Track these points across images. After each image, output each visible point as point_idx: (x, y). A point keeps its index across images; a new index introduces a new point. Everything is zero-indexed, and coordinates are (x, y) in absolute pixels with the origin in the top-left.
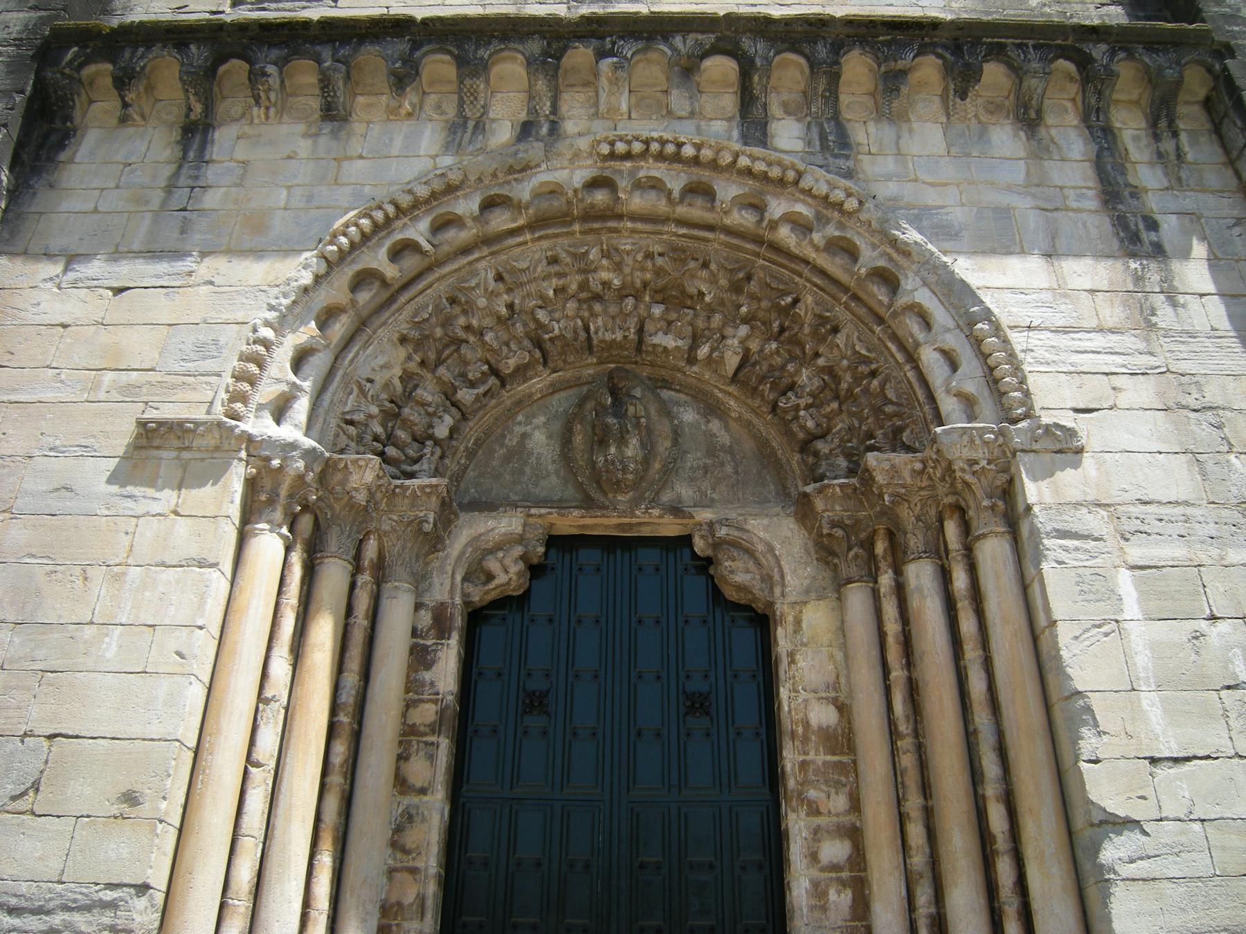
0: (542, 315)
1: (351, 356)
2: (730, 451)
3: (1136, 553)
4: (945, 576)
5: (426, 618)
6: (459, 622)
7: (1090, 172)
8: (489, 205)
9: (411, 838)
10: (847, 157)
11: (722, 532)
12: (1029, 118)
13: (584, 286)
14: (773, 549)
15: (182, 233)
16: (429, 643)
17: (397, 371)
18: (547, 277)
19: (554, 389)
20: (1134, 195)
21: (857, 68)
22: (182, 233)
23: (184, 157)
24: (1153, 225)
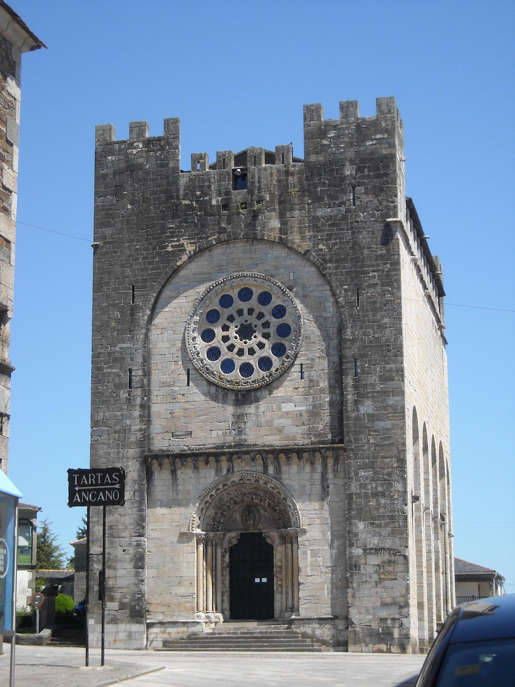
0: (236, 498)
3: (311, 548)
5: (223, 550)
7: (321, 475)
8: (224, 485)
9: (224, 583)
11: (266, 534)
14: (273, 536)
19: (240, 507)
20: (327, 480)
21: (282, 456)
24: (328, 487)
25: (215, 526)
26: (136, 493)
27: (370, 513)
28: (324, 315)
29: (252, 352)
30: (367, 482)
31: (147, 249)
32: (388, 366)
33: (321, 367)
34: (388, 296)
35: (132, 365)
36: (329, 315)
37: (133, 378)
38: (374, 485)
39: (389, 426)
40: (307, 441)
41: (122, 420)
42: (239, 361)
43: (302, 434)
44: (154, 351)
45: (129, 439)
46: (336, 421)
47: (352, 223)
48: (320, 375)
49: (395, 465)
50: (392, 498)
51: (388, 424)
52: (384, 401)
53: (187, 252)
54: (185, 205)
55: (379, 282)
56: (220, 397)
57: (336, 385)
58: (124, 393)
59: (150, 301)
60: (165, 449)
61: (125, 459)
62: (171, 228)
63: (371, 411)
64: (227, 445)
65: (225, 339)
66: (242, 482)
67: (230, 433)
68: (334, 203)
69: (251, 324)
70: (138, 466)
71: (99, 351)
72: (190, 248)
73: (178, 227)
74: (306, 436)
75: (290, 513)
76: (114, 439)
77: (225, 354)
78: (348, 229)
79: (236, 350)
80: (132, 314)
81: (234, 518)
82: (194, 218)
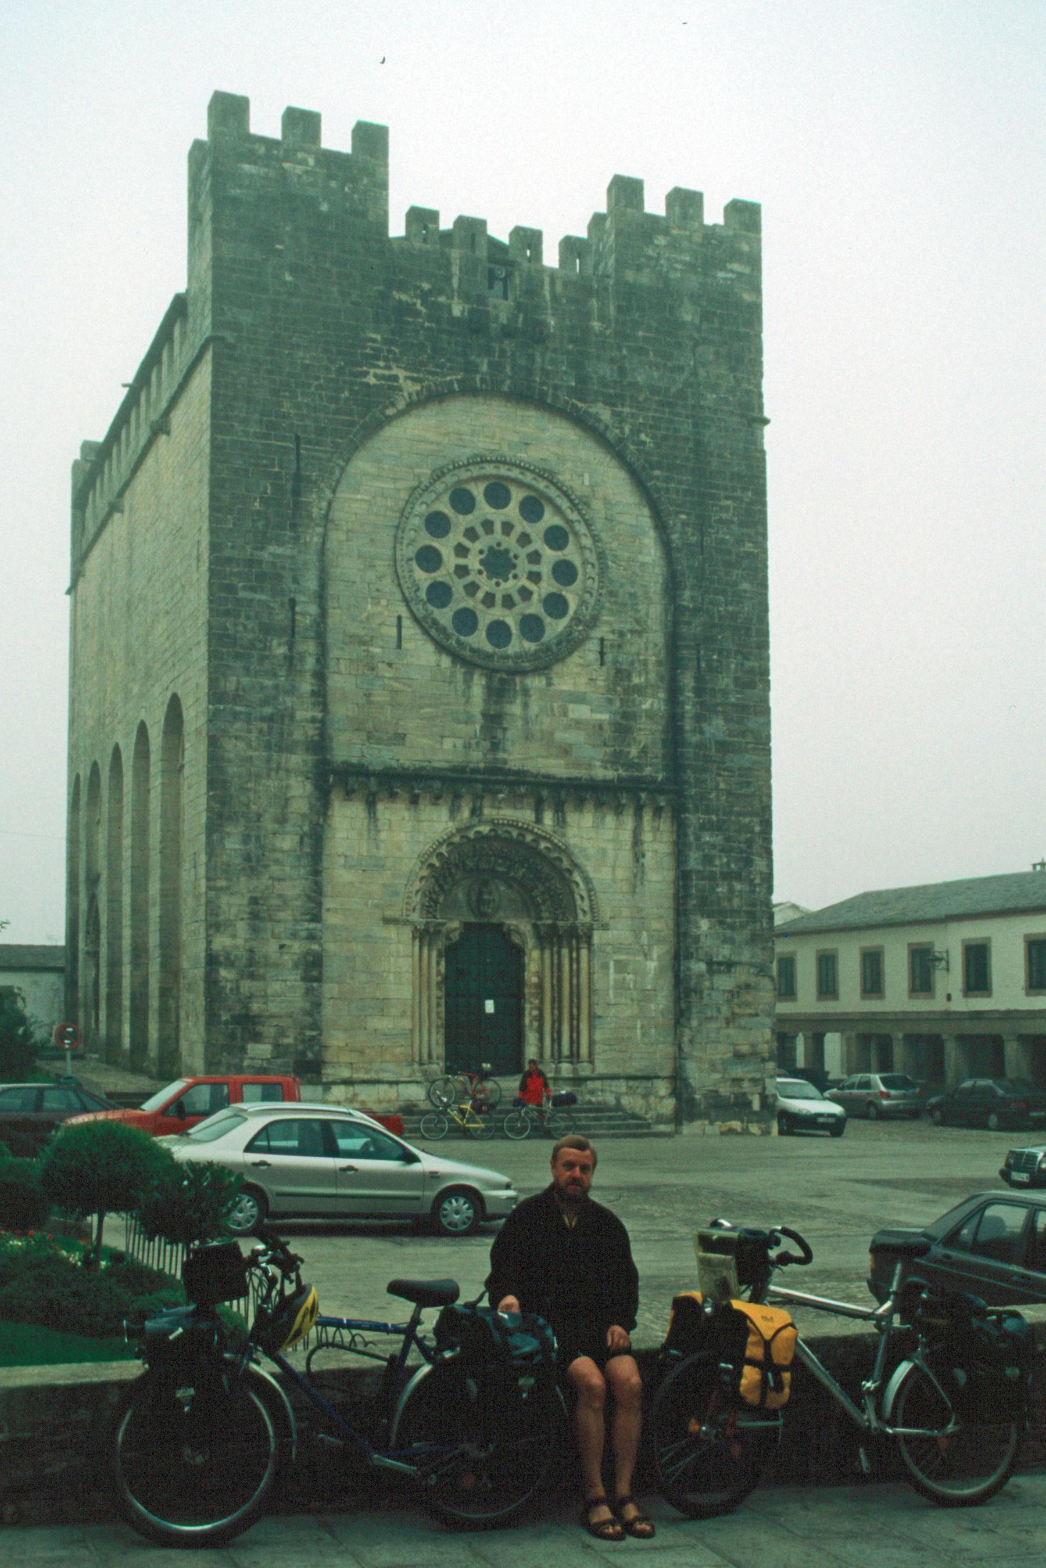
12: (618, 810)
24: (644, 856)
26: (306, 840)
27: (719, 905)
28: (641, 558)
29: (508, 602)
30: (714, 852)
31: (328, 370)
32: (748, 664)
33: (634, 649)
34: (749, 547)
35: (296, 592)
36: (648, 559)
37: (298, 617)
38: (725, 860)
39: (747, 765)
40: (610, 774)
41: (275, 698)
42: (487, 617)
43: (603, 761)
44: (335, 572)
45: (291, 734)
46: (660, 745)
47: (694, 407)
48: (632, 663)
49: (757, 829)
50: (751, 882)
51: (745, 760)
52: (740, 722)
53: (406, 394)
54: (400, 301)
55: (735, 519)
56: (460, 677)
57: (660, 684)
58: (279, 645)
59: (332, 473)
60: (354, 760)
61: (282, 774)
62: (374, 341)
63: (721, 736)
64: (472, 766)
65: (462, 571)
66: (492, 834)
67: (477, 744)
68: (665, 365)
69: (507, 551)
70: (309, 787)
71: (227, 553)
72: (410, 388)
73: (385, 341)
74: (609, 766)
75: (577, 897)
76: (261, 731)
77: (461, 601)
78: (687, 417)
79: (480, 595)
80: (296, 493)
82: (417, 332)
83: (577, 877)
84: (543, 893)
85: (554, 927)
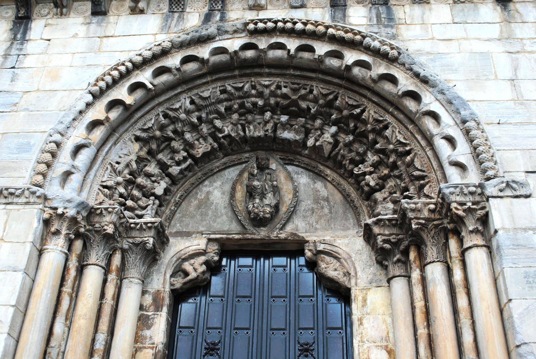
0: (218, 123)
1: (106, 149)
2: (327, 200)
4: (449, 271)
5: (148, 300)
6: (167, 301)
10: (392, 27)
11: (321, 247)
13: (242, 106)
15: (12, 81)
16: (150, 314)
17: (134, 157)
18: (220, 101)
22: (12, 81)
23: (15, 39)
25: (129, 203)
66: (250, 54)
81: (201, 196)
83: (430, 101)
84: (376, 166)
85: (402, 221)
